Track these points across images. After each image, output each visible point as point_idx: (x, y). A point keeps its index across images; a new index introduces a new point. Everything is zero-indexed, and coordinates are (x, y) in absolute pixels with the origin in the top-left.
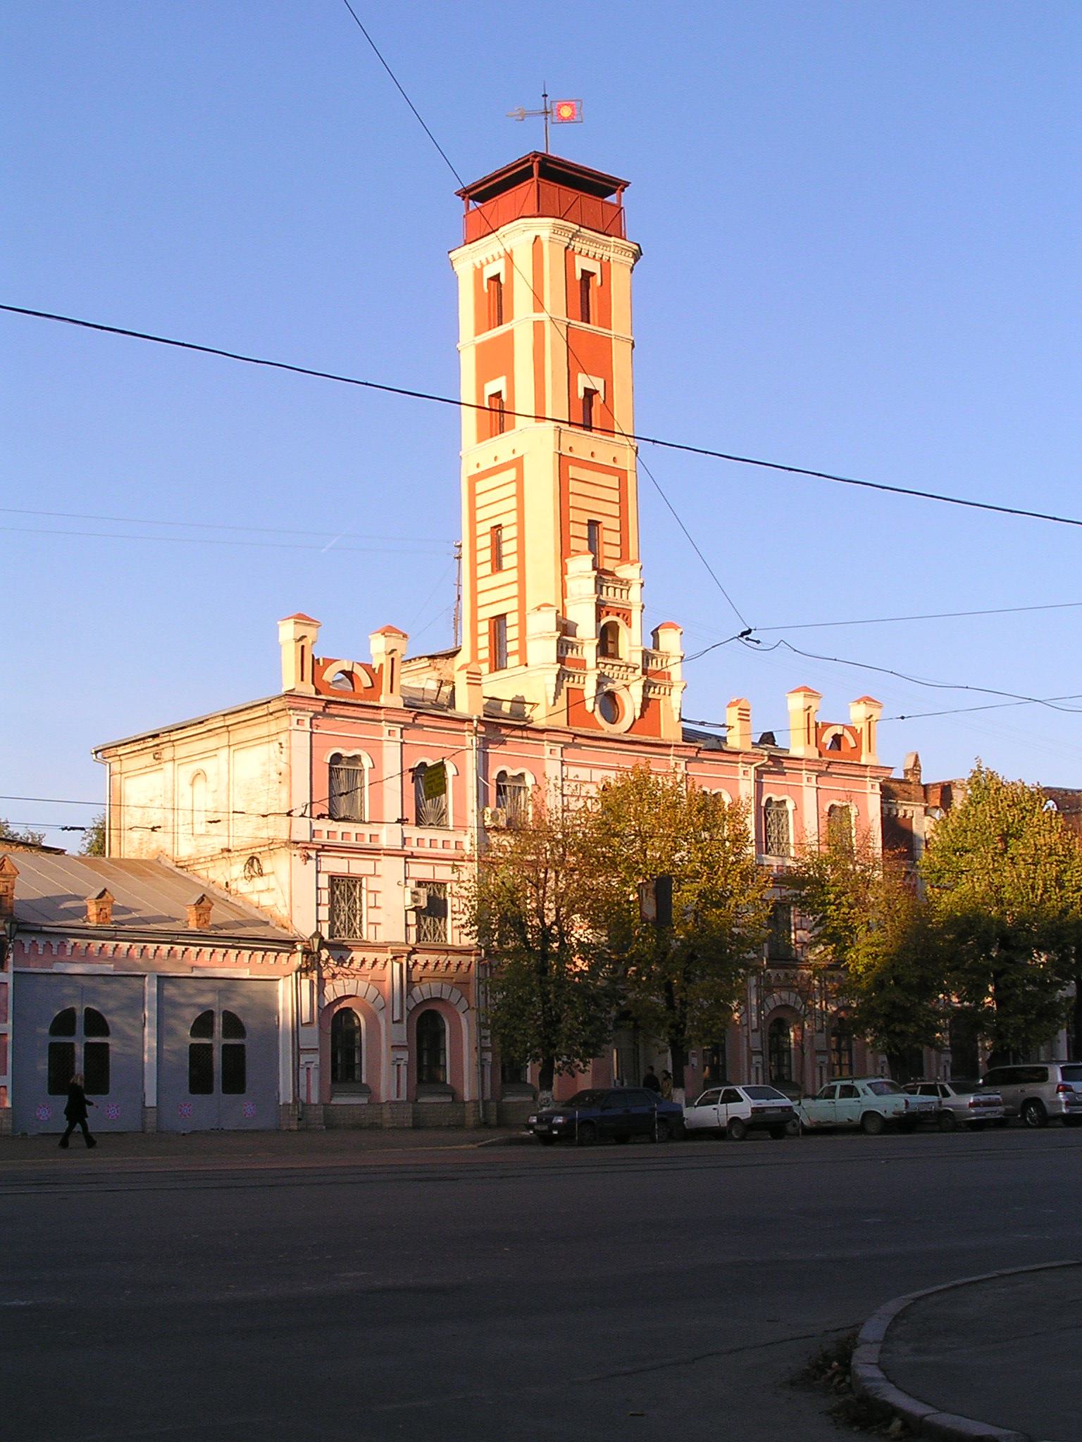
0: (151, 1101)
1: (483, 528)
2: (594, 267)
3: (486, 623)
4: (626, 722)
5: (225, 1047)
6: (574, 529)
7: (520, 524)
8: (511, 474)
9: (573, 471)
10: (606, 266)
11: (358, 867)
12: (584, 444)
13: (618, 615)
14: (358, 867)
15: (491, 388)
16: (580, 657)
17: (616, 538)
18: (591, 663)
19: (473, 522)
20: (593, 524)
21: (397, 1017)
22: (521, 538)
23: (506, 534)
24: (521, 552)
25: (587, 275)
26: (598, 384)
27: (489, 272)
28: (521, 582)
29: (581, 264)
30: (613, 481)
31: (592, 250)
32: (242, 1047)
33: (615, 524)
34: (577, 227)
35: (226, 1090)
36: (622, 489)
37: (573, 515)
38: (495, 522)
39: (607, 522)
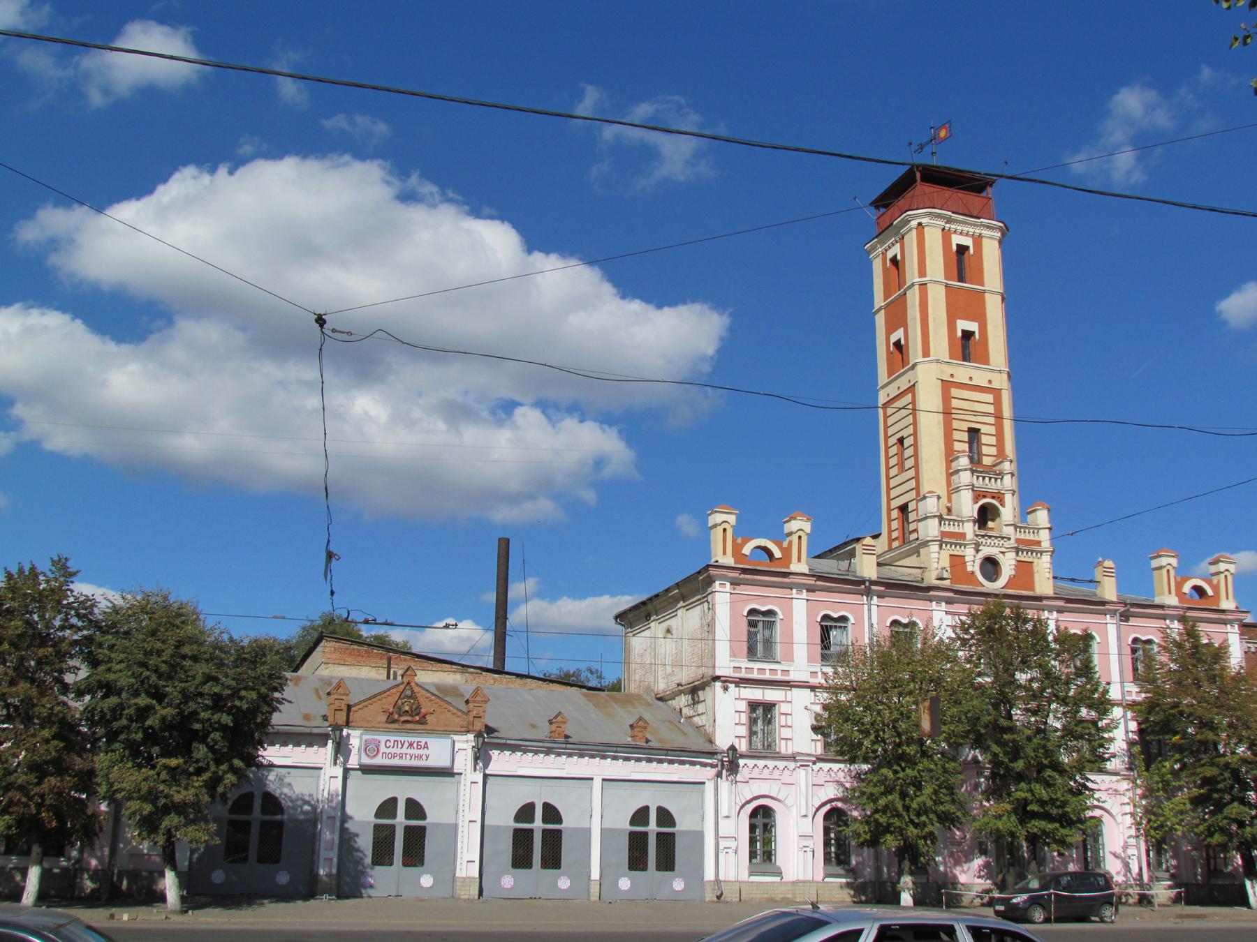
0: (595, 874)
1: (893, 441)
2: (968, 242)
3: (896, 510)
4: (1003, 580)
5: (659, 835)
6: (957, 435)
7: (915, 434)
8: (909, 398)
9: (955, 392)
10: (978, 240)
11: (771, 695)
12: (964, 372)
13: (993, 498)
14: (771, 695)
15: (893, 338)
16: (961, 531)
17: (993, 440)
18: (970, 536)
19: (887, 437)
20: (974, 433)
21: (804, 813)
22: (915, 445)
23: (907, 443)
24: (916, 455)
25: (962, 249)
26: (972, 326)
27: (890, 255)
28: (917, 477)
29: (956, 240)
30: (989, 398)
31: (965, 229)
32: (672, 835)
33: (992, 430)
34: (950, 213)
35: (659, 868)
36: (997, 403)
37: (956, 424)
38: (898, 436)
39: (984, 429)
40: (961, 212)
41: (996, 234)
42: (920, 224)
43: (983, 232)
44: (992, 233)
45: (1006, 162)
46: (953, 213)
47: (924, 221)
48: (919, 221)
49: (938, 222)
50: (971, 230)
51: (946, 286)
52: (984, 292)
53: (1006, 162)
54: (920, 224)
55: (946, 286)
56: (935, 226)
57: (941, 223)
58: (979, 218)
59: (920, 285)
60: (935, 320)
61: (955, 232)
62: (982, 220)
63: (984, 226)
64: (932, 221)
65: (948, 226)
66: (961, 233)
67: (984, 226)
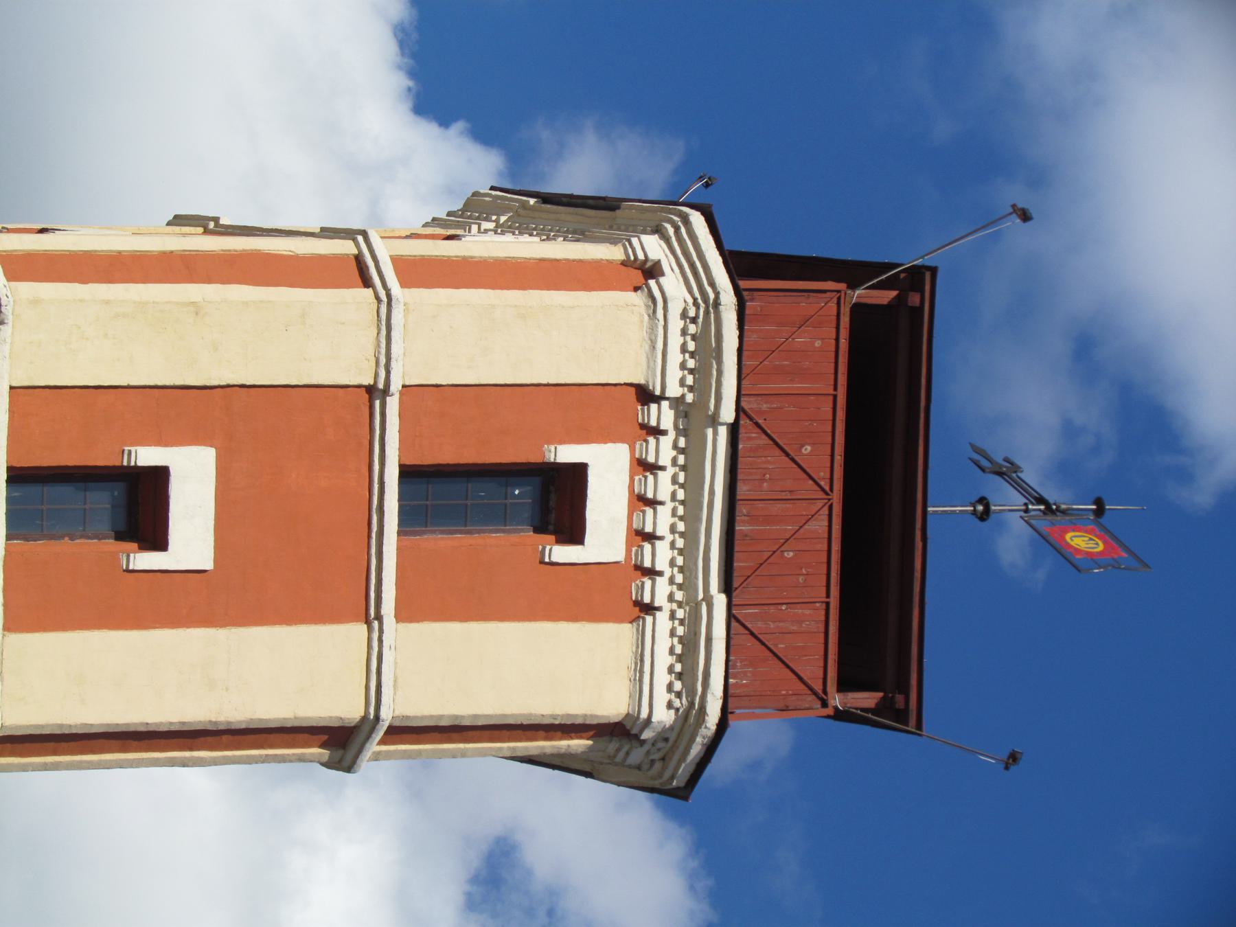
31: (662, 520)
34: (728, 413)
40: (742, 490)
41: (662, 697)
42: (652, 271)
43: (662, 618)
44: (662, 678)
45: (1014, 757)
46: (734, 429)
47: (673, 284)
48: (668, 264)
49: (675, 357)
50: (662, 556)
51: (370, 390)
52: (370, 617)
53: (1014, 757)
54: (652, 271)
55: (374, 393)
56: (657, 348)
57: (674, 374)
58: (727, 587)
59: (359, 259)
60: (197, 309)
61: (646, 467)
62: (720, 601)
63: (692, 621)
64: (676, 324)
65: (665, 416)
66: (642, 501)
67: (692, 621)
